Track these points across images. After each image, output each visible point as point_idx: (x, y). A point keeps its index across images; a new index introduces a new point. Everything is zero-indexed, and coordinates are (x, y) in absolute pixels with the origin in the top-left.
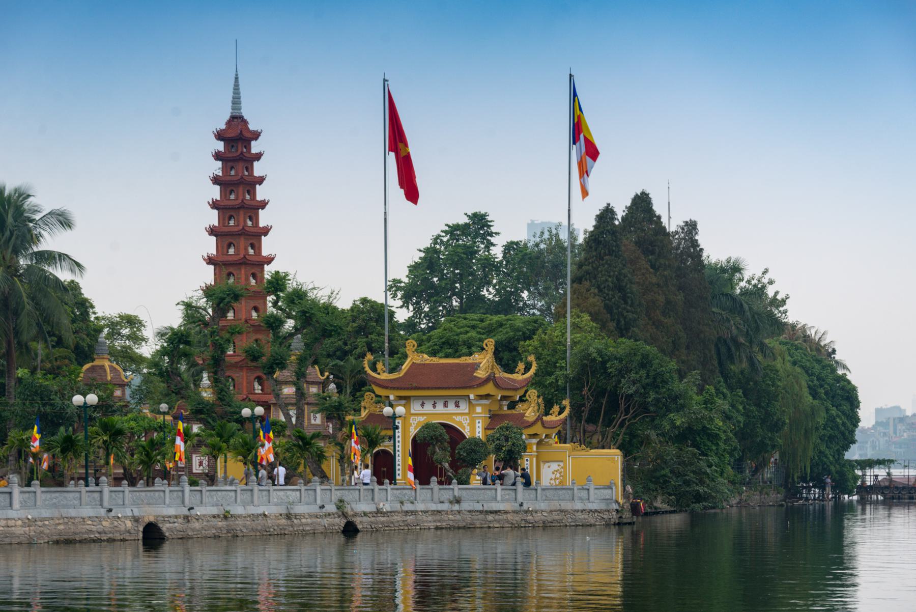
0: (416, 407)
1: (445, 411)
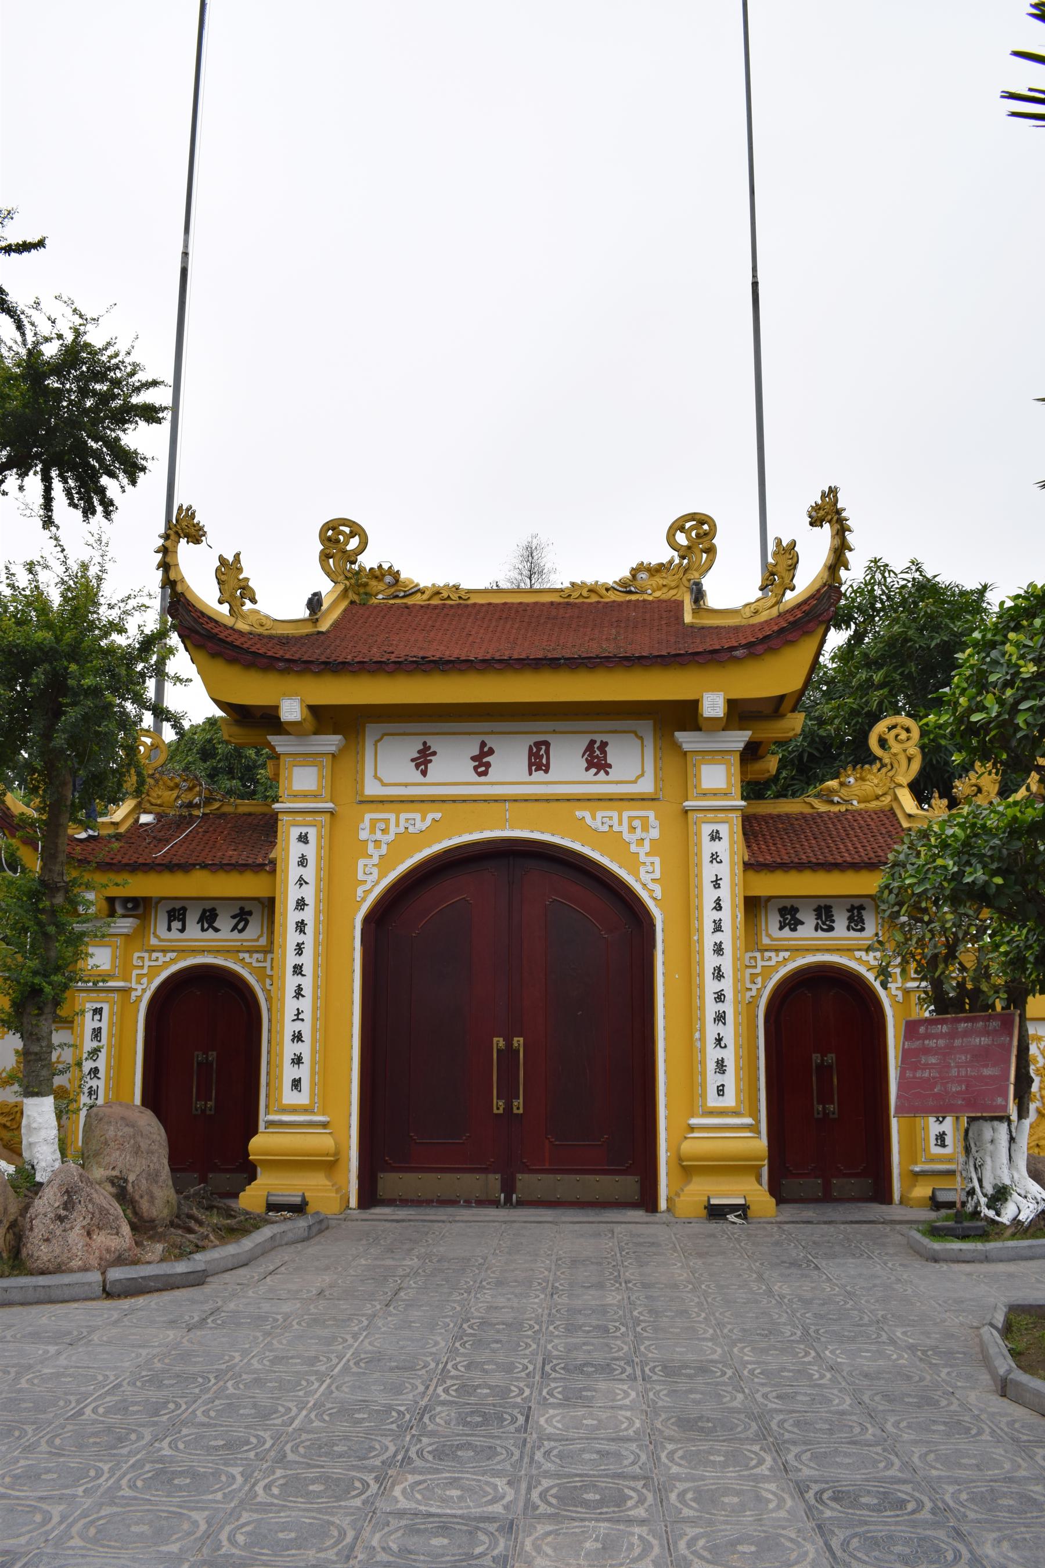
0: (387, 768)
1: (539, 785)
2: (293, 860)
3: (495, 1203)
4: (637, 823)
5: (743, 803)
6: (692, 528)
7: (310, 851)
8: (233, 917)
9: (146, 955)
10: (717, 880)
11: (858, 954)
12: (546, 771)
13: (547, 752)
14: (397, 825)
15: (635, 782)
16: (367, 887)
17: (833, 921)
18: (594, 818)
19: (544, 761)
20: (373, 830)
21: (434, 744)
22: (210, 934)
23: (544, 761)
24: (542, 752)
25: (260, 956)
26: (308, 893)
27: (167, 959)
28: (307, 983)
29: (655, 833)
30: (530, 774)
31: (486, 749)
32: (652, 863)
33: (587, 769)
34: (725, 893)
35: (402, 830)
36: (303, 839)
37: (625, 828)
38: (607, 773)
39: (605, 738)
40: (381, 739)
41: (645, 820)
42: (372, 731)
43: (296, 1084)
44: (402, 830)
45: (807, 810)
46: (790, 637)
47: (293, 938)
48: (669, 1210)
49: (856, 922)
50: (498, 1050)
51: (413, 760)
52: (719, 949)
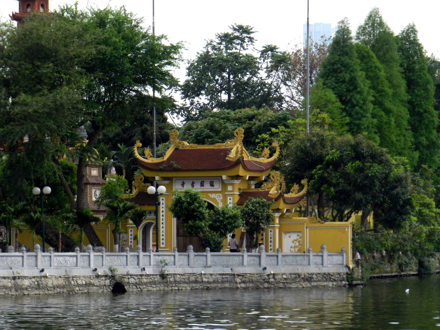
21: (185, 181)
28: (164, 226)
29: (221, 198)
36: (163, 200)
41: (220, 196)
43: (163, 243)
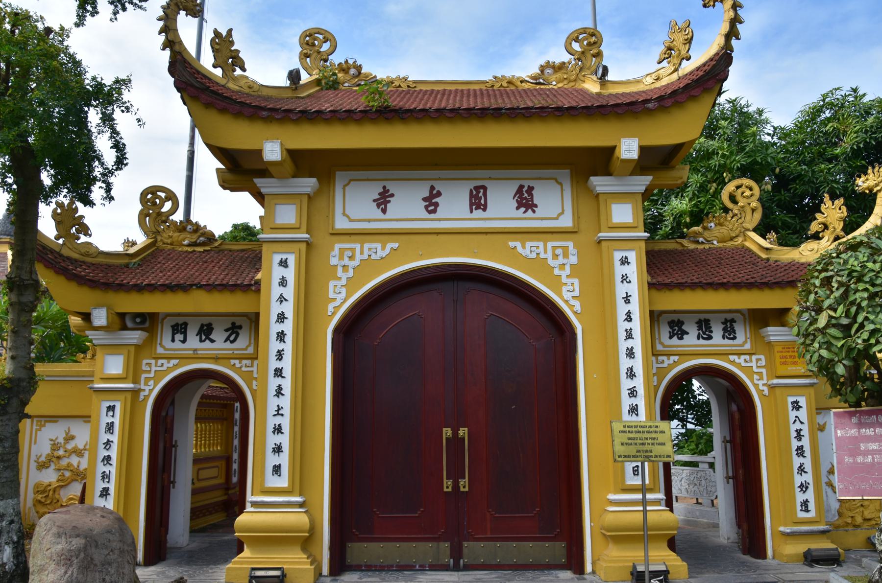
0: (354, 206)
1: (478, 221)
2: (276, 281)
3: (445, 568)
4: (559, 251)
5: (647, 234)
6: (584, 39)
7: (290, 274)
8: (226, 330)
9: (153, 362)
10: (627, 296)
11: (732, 358)
12: (485, 210)
13: (485, 194)
14: (362, 253)
15: (557, 218)
16: (337, 304)
17: (711, 332)
18: (524, 247)
19: (483, 202)
20: (341, 258)
21: (392, 187)
22: (207, 344)
23: (483, 202)
24: (481, 194)
25: (248, 362)
26: (288, 309)
27: (171, 365)
29: (574, 260)
30: (471, 212)
31: (435, 192)
32: (573, 284)
33: (518, 208)
34: (635, 307)
35: (366, 257)
36: (284, 264)
37: (549, 255)
38: (534, 212)
39: (531, 183)
40: (348, 184)
42: (340, 177)
44: (366, 257)
45: (680, 248)
46: (693, 93)
47: (275, 346)
48: (594, 572)
49: (729, 332)
50: (447, 439)
51: (374, 201)
52: (630, 353)
